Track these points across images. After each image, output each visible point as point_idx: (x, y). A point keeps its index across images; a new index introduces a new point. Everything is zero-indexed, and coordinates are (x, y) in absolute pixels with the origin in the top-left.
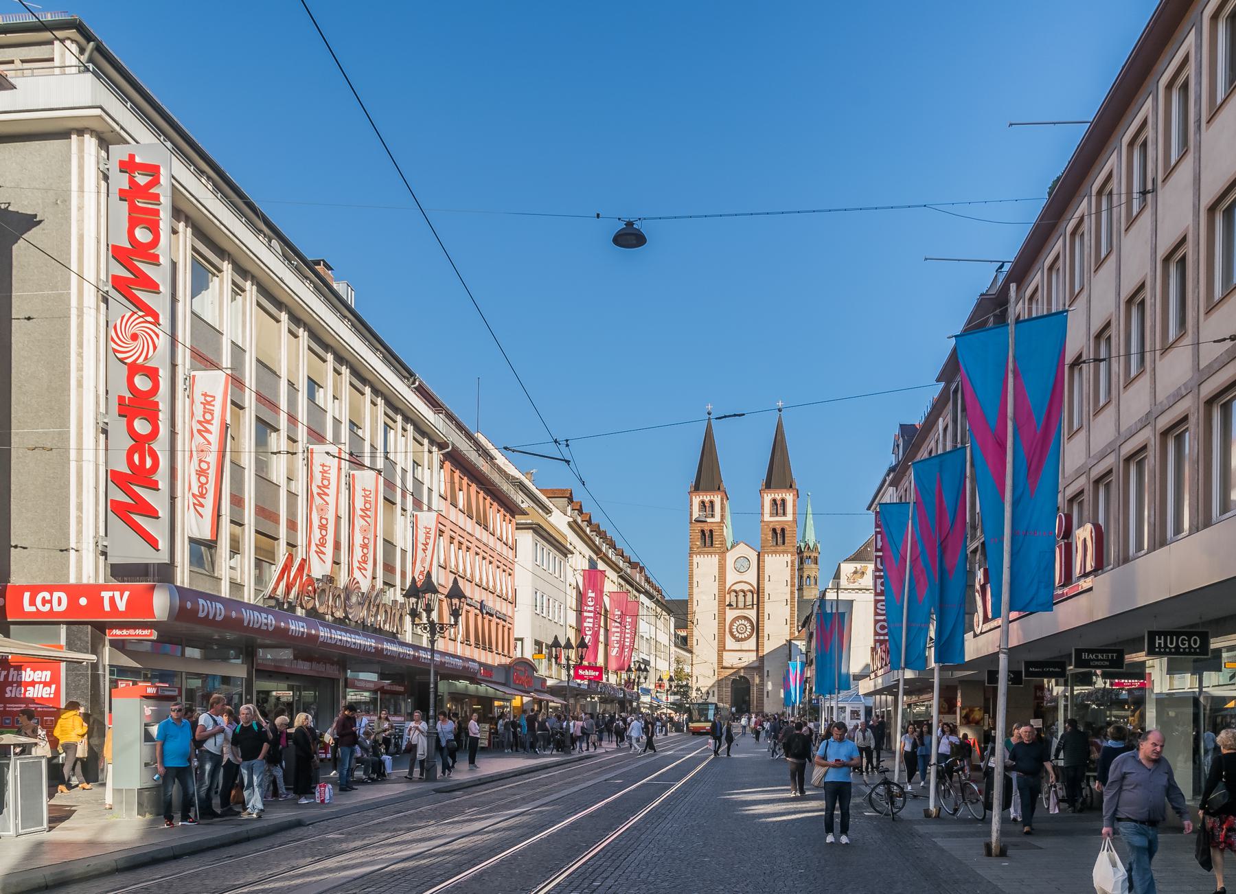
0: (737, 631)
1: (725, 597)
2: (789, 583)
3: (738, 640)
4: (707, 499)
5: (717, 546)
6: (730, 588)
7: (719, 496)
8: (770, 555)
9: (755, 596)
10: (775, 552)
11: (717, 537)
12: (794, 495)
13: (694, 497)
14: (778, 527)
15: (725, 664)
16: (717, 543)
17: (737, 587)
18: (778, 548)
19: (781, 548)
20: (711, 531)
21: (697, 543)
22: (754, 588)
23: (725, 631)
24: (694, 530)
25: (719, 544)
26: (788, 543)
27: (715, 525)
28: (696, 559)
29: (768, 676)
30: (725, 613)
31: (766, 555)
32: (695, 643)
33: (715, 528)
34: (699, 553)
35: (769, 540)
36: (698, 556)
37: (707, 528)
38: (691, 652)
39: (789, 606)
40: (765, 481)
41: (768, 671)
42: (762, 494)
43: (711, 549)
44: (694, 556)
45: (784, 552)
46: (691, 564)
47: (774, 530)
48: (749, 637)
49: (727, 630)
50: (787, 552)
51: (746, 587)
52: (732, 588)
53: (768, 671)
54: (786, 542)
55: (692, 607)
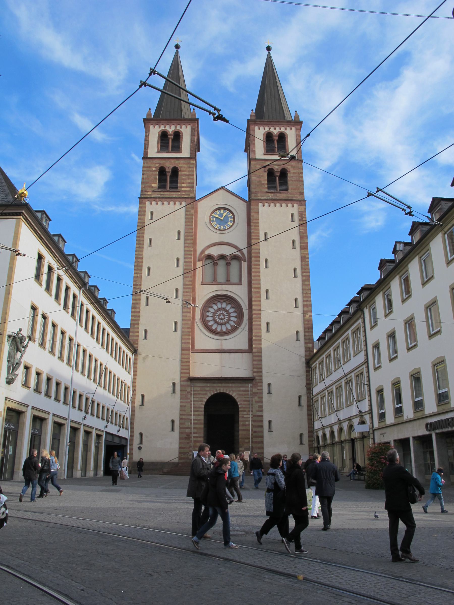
0: (216, 322)
1: (195, 264)
2: (297, 244)
3: (214, 332)
4: (171, 129)
5: (183, 189)
6: (203, 252)
7: (189, 127)
8: (266, 205)
9: (245, 265)
10: (274, 200)
11: (183, 177)
12: (296, 129)
13: (151, 127)
14: (276, 167)
15: (196, 372)
16: (183, 185)
17: (215, 252)
18: (278, 195)
19: (283, 196)
20: (175, 171)
21: (153, 185)
22: (242, 253)
23: (194, 318)
24: (150, 167)
25: (187, 187)
26: (292, 189)
27: (182, 161)
28: (150, 207)
29: (269, 393)
30: (194, 290)
31: (260, 204)
32: (141, 335)
33: (180, 165)
34: (155, 199)
35: (263, 184)
36: (154, 203)
37: (169, 166)
38: (135, 351)
39: (299, 279)
40: (254, 111)
41: (269, 385)
42: (252, 127)
43: (174, 194)
44: (148, 203)
45: (287, 201)
46: (142, 213)
47: (271, 173)
48: (234, 329)
49: (198, 316)
50: (291, 201)
51: (228, 251)
52: (207, 252)
53: (269, 385)
54: (290, 187)
55: (141, 277)
